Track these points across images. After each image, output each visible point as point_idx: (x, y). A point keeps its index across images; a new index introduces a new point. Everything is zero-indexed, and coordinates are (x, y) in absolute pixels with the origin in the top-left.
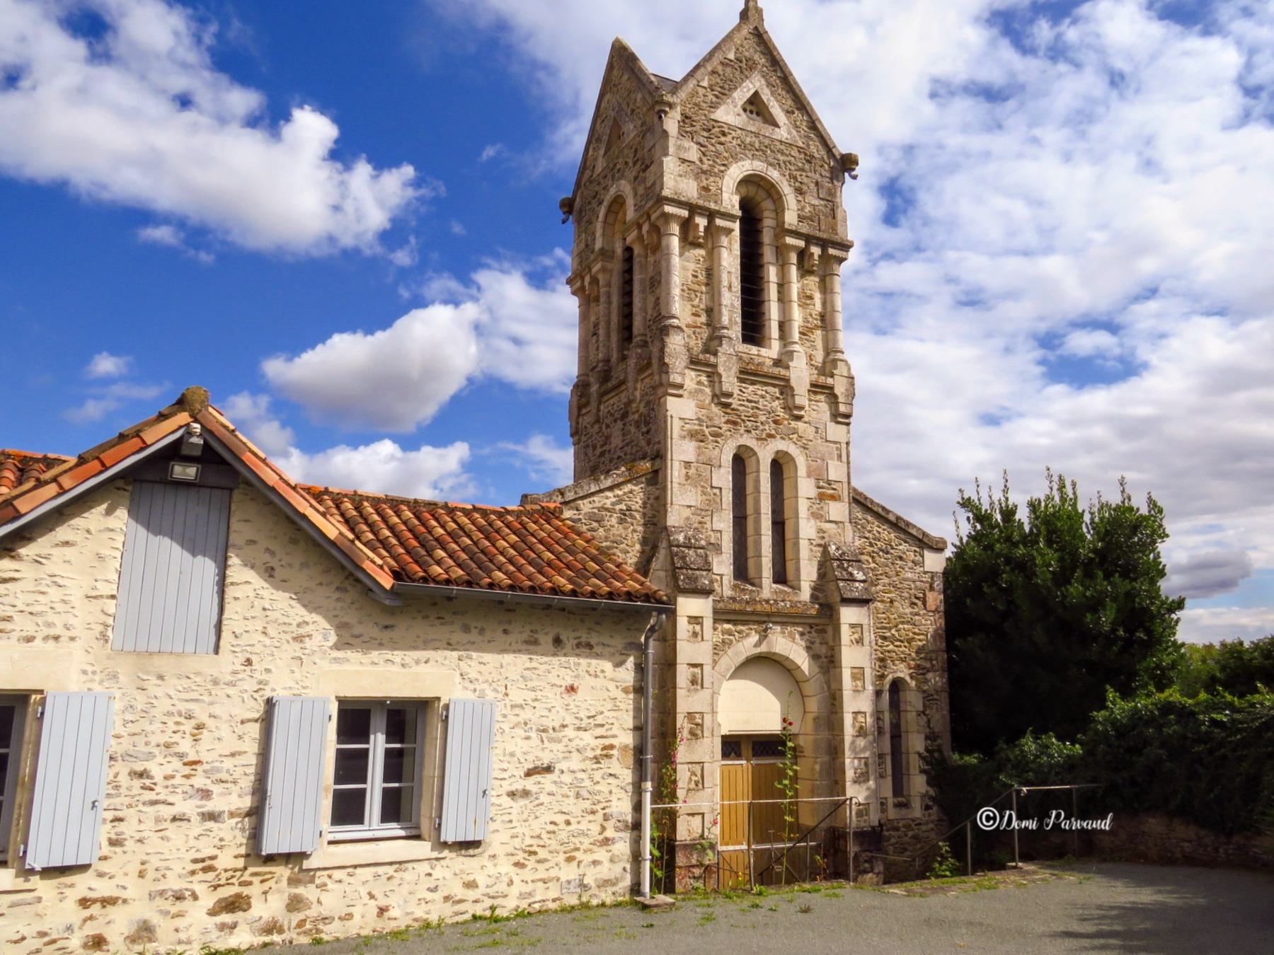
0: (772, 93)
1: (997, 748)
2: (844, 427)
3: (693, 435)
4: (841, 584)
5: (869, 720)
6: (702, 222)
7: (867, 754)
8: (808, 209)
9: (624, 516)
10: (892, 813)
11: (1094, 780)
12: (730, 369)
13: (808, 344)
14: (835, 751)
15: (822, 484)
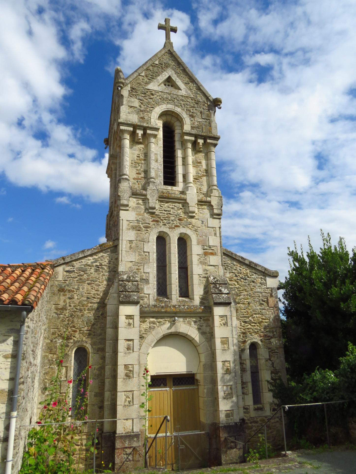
0: (178, 76)
1: (303, 378)
2: (218, 220)
3: (134, 228)
4: (214, 296)
5: (232, 365)
6: (140, 132)
7: (231, 383)
8: (196, 123)
9: (97, 269)
10: (253, 414)
11: (343, 398)
12: (154, 196)
13: (199, 183)
14: (214, 382)
15: (206, 247)
